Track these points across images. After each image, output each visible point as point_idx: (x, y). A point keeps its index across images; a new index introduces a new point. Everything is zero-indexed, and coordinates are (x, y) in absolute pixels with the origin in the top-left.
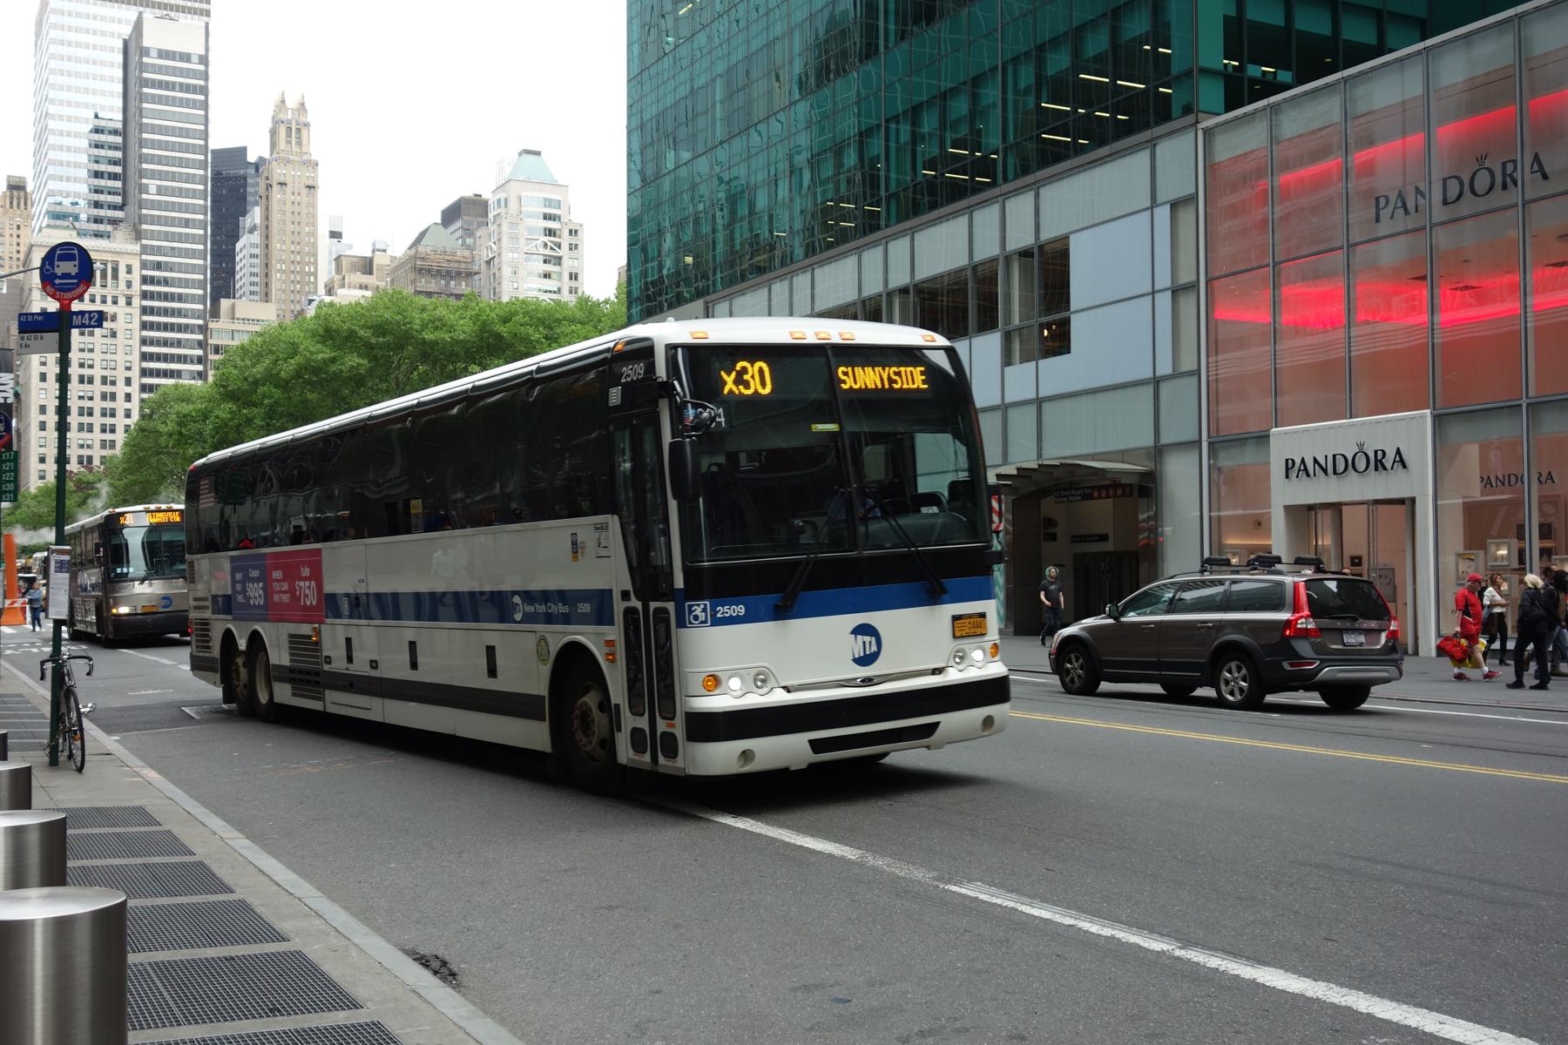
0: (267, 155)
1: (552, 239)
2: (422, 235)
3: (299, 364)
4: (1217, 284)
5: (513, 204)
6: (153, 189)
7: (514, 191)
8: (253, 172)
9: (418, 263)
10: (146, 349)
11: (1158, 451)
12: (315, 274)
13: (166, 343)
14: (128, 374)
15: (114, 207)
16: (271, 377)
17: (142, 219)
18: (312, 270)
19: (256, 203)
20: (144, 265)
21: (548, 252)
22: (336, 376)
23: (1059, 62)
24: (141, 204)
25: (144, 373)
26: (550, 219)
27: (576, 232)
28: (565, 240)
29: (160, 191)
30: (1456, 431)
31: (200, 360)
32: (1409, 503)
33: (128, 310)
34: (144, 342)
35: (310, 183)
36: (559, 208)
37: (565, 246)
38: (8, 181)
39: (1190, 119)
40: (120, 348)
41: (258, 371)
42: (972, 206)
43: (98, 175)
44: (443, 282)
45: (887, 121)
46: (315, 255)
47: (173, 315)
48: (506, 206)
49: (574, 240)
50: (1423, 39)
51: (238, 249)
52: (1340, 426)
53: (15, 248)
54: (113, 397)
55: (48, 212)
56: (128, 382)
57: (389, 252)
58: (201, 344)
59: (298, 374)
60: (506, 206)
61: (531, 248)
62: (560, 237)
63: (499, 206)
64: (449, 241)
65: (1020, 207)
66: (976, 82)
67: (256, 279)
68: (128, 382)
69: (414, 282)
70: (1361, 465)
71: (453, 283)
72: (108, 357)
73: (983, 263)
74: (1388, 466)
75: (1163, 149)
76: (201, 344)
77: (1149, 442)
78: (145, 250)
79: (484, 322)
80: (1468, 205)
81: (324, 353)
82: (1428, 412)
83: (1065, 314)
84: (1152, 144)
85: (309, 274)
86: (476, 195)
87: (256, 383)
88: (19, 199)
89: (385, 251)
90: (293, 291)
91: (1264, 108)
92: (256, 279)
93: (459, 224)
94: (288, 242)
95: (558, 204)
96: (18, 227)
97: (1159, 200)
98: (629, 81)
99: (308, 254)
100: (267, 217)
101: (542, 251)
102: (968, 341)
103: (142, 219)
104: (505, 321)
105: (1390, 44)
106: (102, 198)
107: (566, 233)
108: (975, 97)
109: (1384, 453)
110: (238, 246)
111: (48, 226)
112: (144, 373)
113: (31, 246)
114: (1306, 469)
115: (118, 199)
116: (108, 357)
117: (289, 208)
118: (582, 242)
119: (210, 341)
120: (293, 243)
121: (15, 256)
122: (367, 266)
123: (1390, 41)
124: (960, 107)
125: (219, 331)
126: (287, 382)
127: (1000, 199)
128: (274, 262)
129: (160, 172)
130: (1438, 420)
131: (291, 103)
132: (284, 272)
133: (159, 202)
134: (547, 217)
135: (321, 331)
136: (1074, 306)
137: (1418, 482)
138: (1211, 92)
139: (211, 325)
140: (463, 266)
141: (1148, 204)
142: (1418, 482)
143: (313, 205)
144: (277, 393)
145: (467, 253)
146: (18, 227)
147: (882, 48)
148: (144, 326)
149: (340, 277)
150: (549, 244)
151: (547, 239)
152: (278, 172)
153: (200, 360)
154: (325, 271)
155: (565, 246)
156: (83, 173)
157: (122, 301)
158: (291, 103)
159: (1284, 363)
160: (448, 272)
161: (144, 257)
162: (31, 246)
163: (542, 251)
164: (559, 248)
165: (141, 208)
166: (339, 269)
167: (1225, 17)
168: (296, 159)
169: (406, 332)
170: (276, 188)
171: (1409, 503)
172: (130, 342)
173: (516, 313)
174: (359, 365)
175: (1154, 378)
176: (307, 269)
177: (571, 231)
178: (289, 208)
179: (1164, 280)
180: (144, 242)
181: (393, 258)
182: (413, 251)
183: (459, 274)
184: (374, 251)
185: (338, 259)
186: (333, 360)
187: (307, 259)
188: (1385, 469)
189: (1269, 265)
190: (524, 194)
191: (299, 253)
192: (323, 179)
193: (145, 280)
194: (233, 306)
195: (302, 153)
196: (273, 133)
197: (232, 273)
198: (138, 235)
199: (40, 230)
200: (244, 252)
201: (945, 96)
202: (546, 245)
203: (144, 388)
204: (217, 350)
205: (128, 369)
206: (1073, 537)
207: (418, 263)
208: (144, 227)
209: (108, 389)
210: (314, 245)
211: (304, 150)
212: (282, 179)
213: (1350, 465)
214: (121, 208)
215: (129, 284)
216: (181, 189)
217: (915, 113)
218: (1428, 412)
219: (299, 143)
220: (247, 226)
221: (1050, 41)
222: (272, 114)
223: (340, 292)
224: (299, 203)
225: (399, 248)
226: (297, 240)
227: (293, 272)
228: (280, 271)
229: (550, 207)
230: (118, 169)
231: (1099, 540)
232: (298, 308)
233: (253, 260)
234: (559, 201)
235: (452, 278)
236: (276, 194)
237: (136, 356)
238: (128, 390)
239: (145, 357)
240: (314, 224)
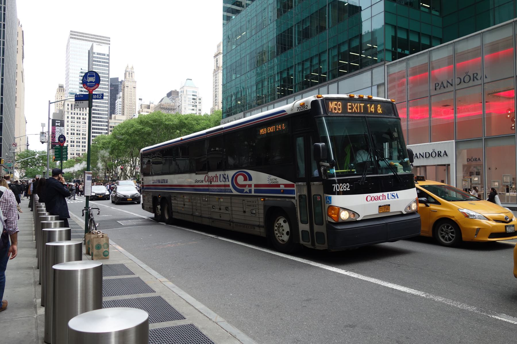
1: (195, 101)
2: (162, 99)
5: (185, 92)
7: (185, 89)
9: (161, 106)
12: (135, 109)
13: (98, 125)
21: (193, 104)
23: (345, 48)
28: (198, 101)
30: (462, 146)
31: (107, 129)
32: (447, 166)
35: (134, 87)
37: (198, 103)
39: (383, 63)
46: (135, 104)
47: (100, 118)
49: (200, 101)
50: (441, 44)
51: (116, 102)
52: (428, 145)
58: (107, 126)
64: (168, 101)
66: (320, 55)
67: (121, 110)
70: (434, 155)
71: (170, 111)
74: (442, 155)
75: (374, 71)
76: (107, 126)
80: (464, 85)
82: (454, 141)
84: (371, 69)
85: (134, 109)
92: (121, 110)
93: (171, 97)
97: (373, 85)
100: (123, 95)
105: (433, 45)
107: (198, 99)
109: (441, 152)
114: (417, 156)
119: (109, 125)
122: (148, 107)
123: (433, 44)
124: (307, 65)
125: (111, 122)
127: (327, 85)
130: (456, 142)
131: (130, 67)
137: (451, 160)
138: (389, 56)
139: (110, 121)
142: (451, 160)
145: (173, 104)
151: (193, 101)
152: (126, 84)
153: (107, 129)
154: (138, 108)
155: (198, 103)
158: (130, 67)
159: (410, 128)
166: (141, 108)
167: (392, 36)
170: (126, 87)
171: (447, 166)
178: (129, 92)
182: (160, 103)
183: (171, 109)
185: (141, 105)
188: (441, 156)
189: (406, 101)
190: (188, 89)
192: (137, 86)
194: (115, 116)
196: (125, 74)
197: (115, 108)
201: (311, 59)
202: (193, 102)
204: (111, 127)
210: (135, 102)
212: (127, 86)
213: (430, 155)
216: (102, 87)
217: (303, 63)
218: (454, 141)
219: (132, 77)
220: (119, 97)
221: (342, 43)
222: (125, 69)
225: (156, 103)
226: (131, 100)
234: (196, 92)
235: (170, 110)
236: (126, 89)
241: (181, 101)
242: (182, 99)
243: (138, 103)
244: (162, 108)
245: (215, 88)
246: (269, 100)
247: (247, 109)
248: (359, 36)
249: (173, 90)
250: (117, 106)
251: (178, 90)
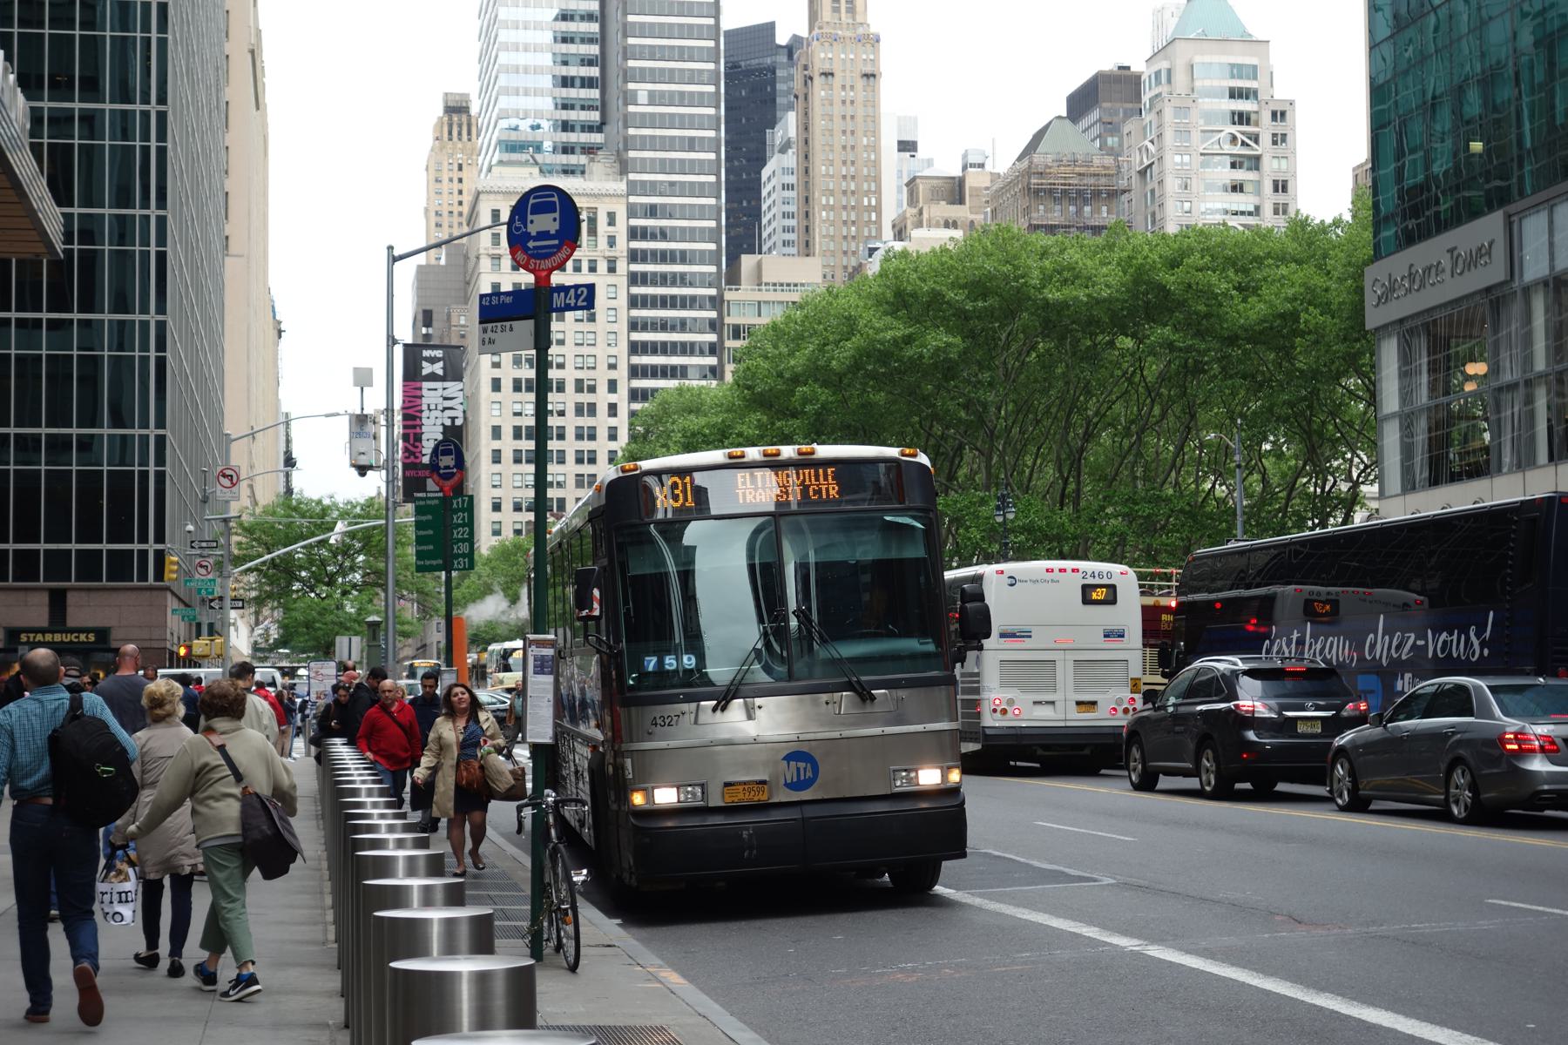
0: (803, 32)
2: (1039, 136)
3: (858, 349)
5: (1180, 78)
6: (643, 97)
7: (1182, 54)
8: (784, 59)
10: (636, 336)
12: (878, 209)
13: (664, 326)
14: (613, 375)
15: (589, 128)
16: (818, 373)
17: (628, 143)
18: (873, 203)
19: (790, 107)
20: (632, 211)
21: (1238, 150)
22: (915, 364)
24: (627, 121)
25: (635, 372)
26: (1240, 96)
27: (1283, 114)
28: (1266, 128)
29: (654, 99)
31: (713, 349)
33: (611, 279)
34: (634, 326)
35: (869, 69)
36: (1255, 78)
37: (1266, 139)
38: (446, 102)
40: (601, 339)
41: (797, 362)
43: (566, 82)
44: (1072, 209)
46: (877, 179)
47: (673, 284)
48: (1169, 81)
49: (1279, 128)
51: (764, 178)
53: (457, 198)
54: (592, 410)
55: (500, 142)
56: (613, 386)
57: (988, 168)
58: (714, 326)
59: (856, 365)
60: (1169, 81)
61: (1210, 145)
62: (1257, 124)
64: (1080, 143)
67: (792, 222)
68: (613, 386)
69: (1027, 211)
71: (1087, 209)
72: (585, 350)
76: (714, 326)
78: (633, 188)
79: (1140, 267)
81: (899, 330)
85: (869, 208)
86: (1120, 68)
87: (796, 380)
88: (460, 126)
89: (982, 166)
90: (845, 238)
92: (792, 222)
93: (1095, 115)
94: (838, 162)
95: (1253, 72)
96: (460, 168)
99: (867, 178)
100: (805, 127)
101: (1228, 148)
103: (628, 143)
104: (1173, 264)
106: (572, 115)
107: (1266, 117)
110: (765, 173)
111: (501, 162)
112: (635, 372)
113: (478, 194)
115: (595, 116)
116: (585, 350)
117: (837, 110)
119: (727, 320)
120: (844, 163)
121: (456, 209)
122: (955, 191)
125: (740, 303)
126: (841, 376)
128: (817, 194)
129: (652, 70)
132: (832, 208)
133: (653, 115)
134: (1235, 94)
135: (889, 295)
139: (728, 296)
140: (1103, 181)
143: (873, 103)
144: (824, 395)
145: (1109, 161)
146: (460, 168)
148: (634, 302)
149: (915, 211)
150: (1239, 136)
151: (1235, 129)
152: (821, 57)
153: (713, 349)
154: (892, 204)
155: (1266, 139)
156: (546, 82)
157: (602, 266)
160: (1079, 192)
161: (632, 199)
162: (478, 194)
163: (1228, 148)
164: (1256, 141)
165: (626, 127)
166: (913, 199)
168: (848, 34)
169: (1018, 290)
170: (818, 81)
172: (614, 327)
173: (1191, 250)
174: (948, 345)
176: (866, 203)
177: (1274, 114)
178: (837, 110)
180: (632, 176)
181: (995, 177)
182: (1025, 163)
183: (1096, 194)
184: (965, 168)
185: (912, 183)
186: (908, 340)
187: (865, 186)
190: (1197, 59)
191: (853, 177)
192: (889, 63)
193: (634, 233)
194: (759, 266)
195: (855, 26)
197: (756, 214)
198: (624, 167)
199: (489, 170)
200: (774, 182)
202: (1234, 139)
203: (635, 395)
204: (737, 332)
205: (612, 367)
207: (1034, 181)
208: (632, 154)
209: (585, 398)
210: (876, 164)
211: (859, 19)
212: (827, 67)
214: (599, 128)
215: (612, 241)
216: (682, 94)
223: (916, 233)
224: (852, 102)
225: (1003, 161)
226: (851, 157)
227: (845, 208)
228: (825, 207)
229: (1240, 77)
230: (594, 72)
232: (853, 262)
233: (787, 194)
234: (1255, 67)
235: (1086, 202)
236: (819, 91)
237: (624, 347)
238: (613, 398)
239: (635, 348)
240: (875, 133)
241: (1160, 136)
242: (1160, 126)
243: (893, 167)
244: (1036, 193)
249: (1108, 65)
250: (769, 202)
251: (1138, 66)
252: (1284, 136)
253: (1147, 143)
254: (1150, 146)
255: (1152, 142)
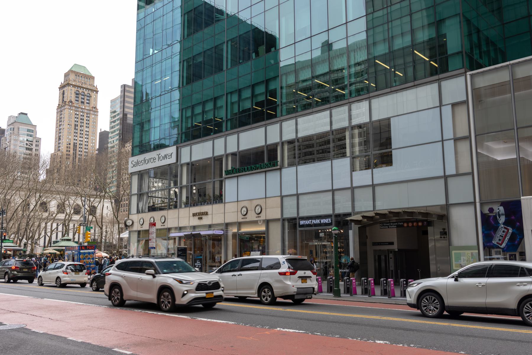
4: (519, 130)
11: (448, 206)
21: (28, 146)
28: (34, 144)
36: (33, 133)
42: (267, 124)
45: (227, 94)
48: (13, 130)
49: (37, 143)
60: (13, 130)
61: (22, 144)
63: (11, 130)
65: (232, 140)
73: (217, 156)
77: (443, 202)
83: (389, 150)
91: (507, 66)
95: (32, 131)
98: (136, 63)
102: (295, 167)
107: (35, 141)
108: (240, 96)
118: (40, 144)
136: (393, 146)
141: (438, 105)
147: (225, 68)
163: (25, 146)
175: (445, 175)
177: (36, 141)
179: (449, 134)
190: (20, 127)
206: (373, 243)
229: (30, 132)
231: (389, 245)
234: (33, 130)
241: (10, 141)
245: (58, 129)
246: (284, 113)
247: (284, 113)
248: (265, 81)
252: (38, 145)
253: (7, 142)
254: (8, 143)
255: (8, 142)
